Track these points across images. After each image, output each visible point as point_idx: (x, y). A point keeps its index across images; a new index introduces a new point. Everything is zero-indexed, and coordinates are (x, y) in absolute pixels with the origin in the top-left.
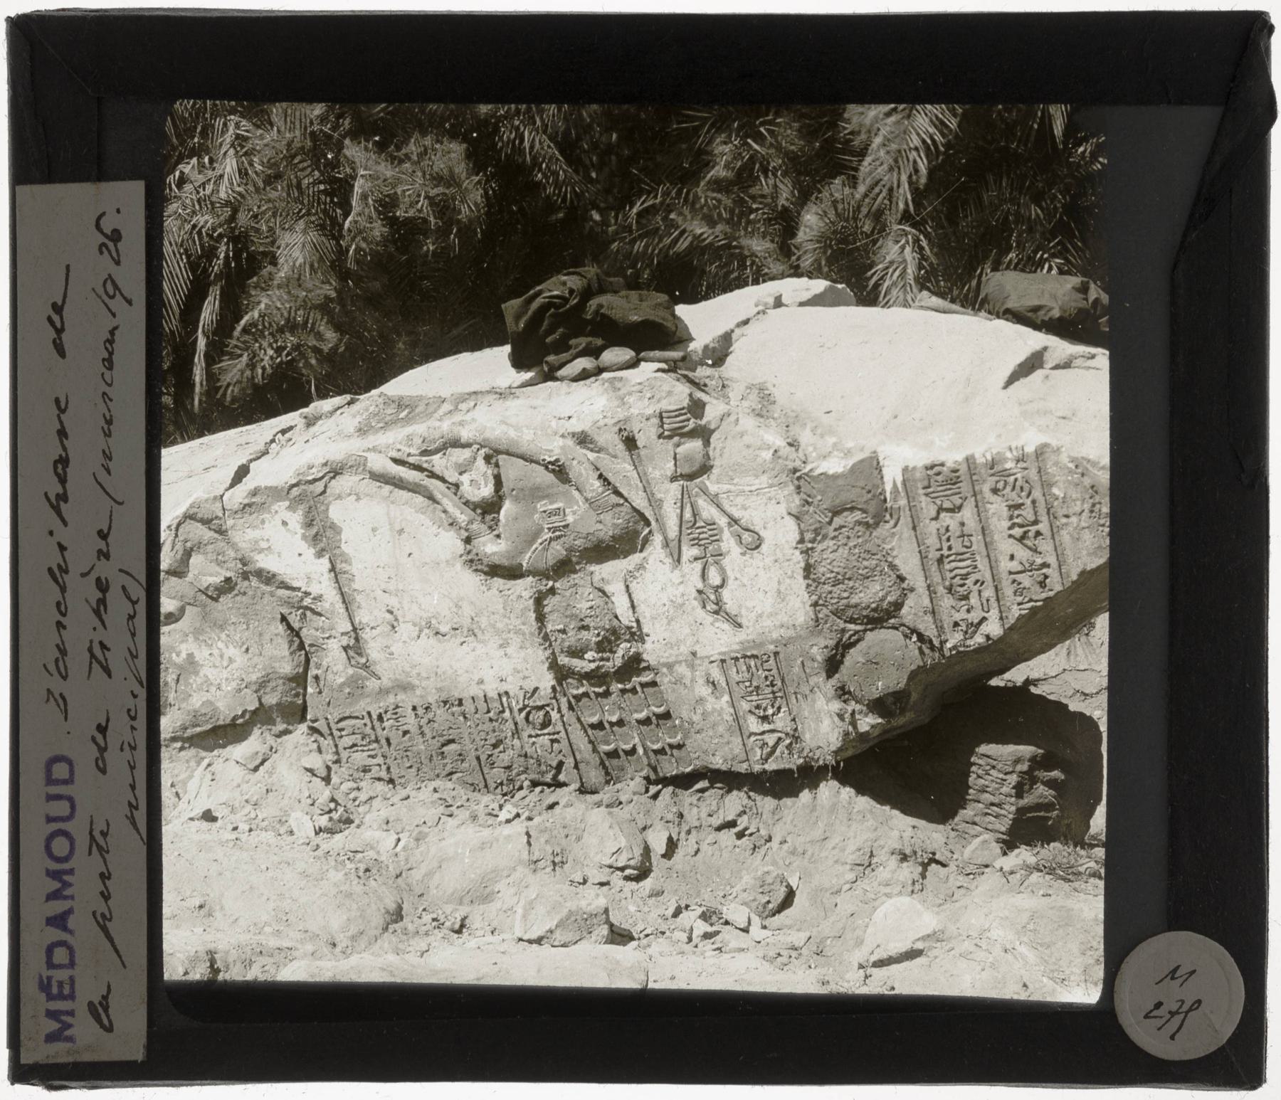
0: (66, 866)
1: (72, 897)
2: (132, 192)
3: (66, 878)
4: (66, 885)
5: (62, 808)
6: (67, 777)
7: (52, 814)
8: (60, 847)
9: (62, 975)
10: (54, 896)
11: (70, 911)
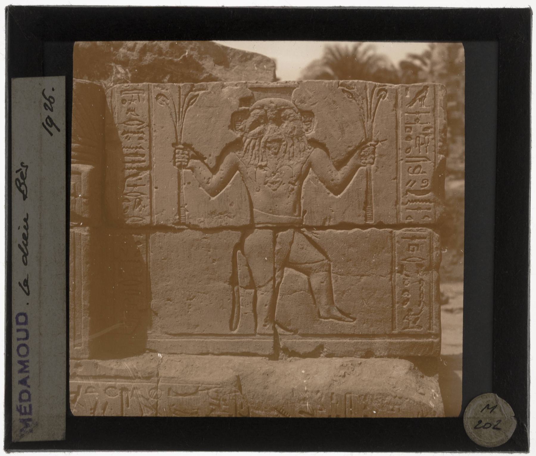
2: (59, 82)
3: (26, 364)
4: (26, 367)
8: (23, 351)
9: (26, 404)
10: (21, 371)
11: (28, 377)
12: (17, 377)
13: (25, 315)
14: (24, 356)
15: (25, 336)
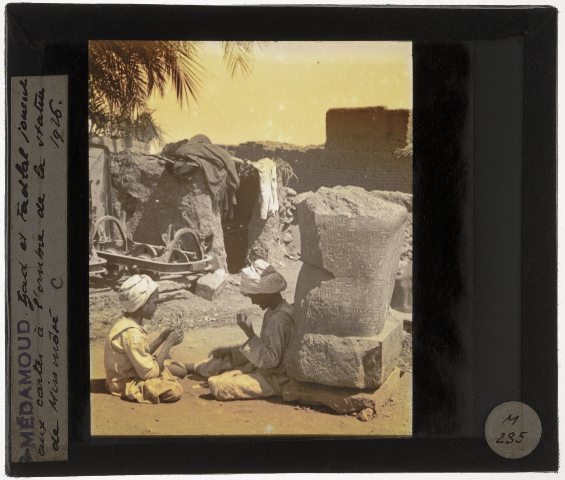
1: (30, 382)
3: (28, 374)
5: (24, 343)
6: (26, 329)
7: (22, 346)
9: (26, 417)
10: (23, 382)
13: (26, 322)
14: (25, 366)
15: (27, 345)
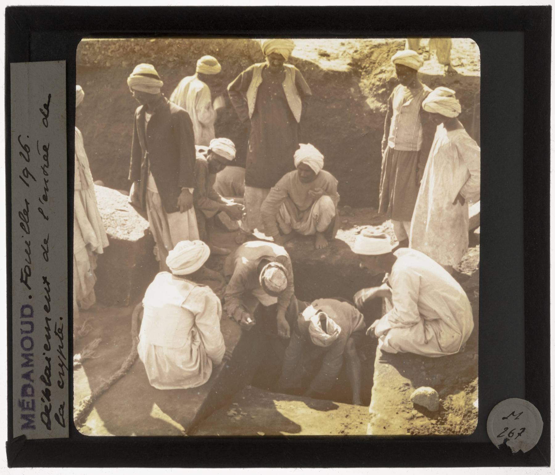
0: (30, 352)
3: (31, 357)
7: (23, 329)
8: (27, 344)
10: (25, 365)
11: (32, 372)
12: (19, 371)
